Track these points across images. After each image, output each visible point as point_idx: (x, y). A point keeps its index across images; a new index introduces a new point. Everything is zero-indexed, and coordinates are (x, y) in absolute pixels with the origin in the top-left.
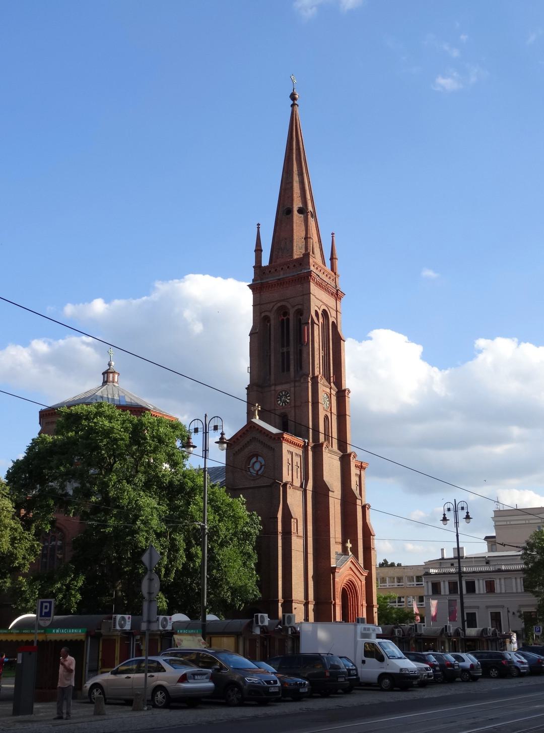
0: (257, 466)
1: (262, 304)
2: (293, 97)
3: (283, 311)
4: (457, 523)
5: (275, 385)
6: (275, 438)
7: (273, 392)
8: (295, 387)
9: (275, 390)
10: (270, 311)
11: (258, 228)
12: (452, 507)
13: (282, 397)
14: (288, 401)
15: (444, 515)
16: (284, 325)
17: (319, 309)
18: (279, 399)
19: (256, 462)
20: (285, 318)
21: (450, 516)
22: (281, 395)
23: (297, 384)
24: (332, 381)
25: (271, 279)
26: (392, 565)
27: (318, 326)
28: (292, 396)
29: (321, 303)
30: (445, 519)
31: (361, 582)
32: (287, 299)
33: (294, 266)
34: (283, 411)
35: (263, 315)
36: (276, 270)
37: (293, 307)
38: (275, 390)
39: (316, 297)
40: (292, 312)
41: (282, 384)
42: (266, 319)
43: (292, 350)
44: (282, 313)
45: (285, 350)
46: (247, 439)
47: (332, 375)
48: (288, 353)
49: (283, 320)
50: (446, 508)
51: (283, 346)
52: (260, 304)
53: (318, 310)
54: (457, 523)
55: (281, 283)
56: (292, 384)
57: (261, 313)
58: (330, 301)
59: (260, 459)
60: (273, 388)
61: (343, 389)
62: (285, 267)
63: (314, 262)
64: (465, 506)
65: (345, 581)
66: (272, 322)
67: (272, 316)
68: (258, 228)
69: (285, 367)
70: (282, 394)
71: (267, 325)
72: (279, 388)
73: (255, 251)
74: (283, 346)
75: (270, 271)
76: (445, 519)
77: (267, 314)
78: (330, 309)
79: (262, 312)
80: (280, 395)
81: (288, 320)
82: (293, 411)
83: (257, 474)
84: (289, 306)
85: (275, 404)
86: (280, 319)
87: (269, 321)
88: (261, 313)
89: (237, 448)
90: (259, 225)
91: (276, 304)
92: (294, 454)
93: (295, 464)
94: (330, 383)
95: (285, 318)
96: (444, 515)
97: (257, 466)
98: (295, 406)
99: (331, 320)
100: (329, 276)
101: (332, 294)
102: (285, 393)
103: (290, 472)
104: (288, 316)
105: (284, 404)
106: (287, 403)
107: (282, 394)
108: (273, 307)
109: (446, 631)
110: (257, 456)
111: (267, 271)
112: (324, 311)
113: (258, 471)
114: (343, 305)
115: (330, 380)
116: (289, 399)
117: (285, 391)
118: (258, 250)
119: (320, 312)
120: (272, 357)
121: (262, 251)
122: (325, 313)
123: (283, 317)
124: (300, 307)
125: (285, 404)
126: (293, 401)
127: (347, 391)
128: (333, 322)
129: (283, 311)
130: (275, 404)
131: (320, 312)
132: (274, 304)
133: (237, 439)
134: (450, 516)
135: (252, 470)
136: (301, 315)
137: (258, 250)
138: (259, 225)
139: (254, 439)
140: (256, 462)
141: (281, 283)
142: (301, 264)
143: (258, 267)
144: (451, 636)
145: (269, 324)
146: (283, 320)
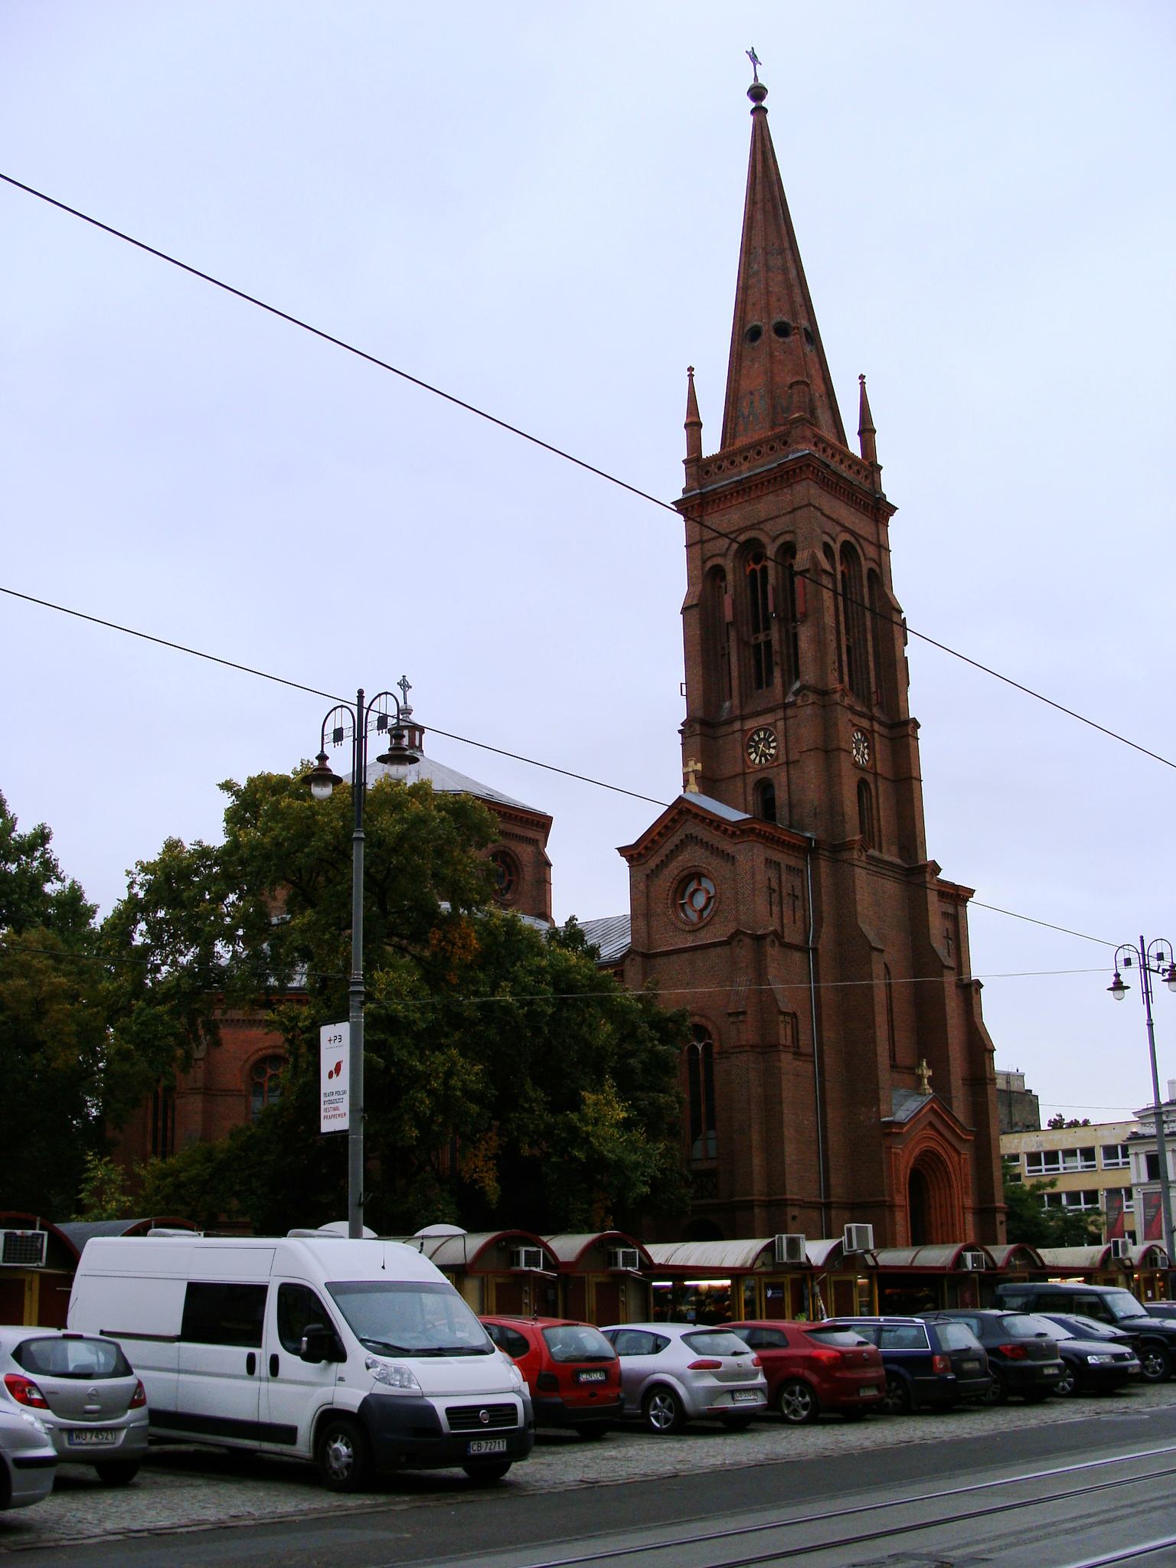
0: (700, 900)
1: (707, 541)
2: (757, 93)
3: (752, 550)
4: (1147, 993)
5: (743, 718)
6: (734, 833)
7: (738, 735)
8: (785, 719)
9: (742, 730)
10: (724, 555)
11: (691, 376)
12: (1134, 956)
13: (757, 743)
15: (1117, 975)
16: (756, 582)
17: (834, 540)
19: (696, 891)
20: (758, 567)
21: (1132, 977)
23: (790, 712)
24: (874, 702)
25: (721, 482)
26: (1074, 1124)
28: (781, 739)
29: (838, 528)
30: (1118, 986)
31: (959, 1154)
32: (759, 523)
33: (772, 448)
34: (761, 775)
35: (709, 564)
36: (732, 463)
37: (774, 540)
38: (742, 730)
39: (823, 514)
40: (771, 551)
41: (758, 714)
43: (775, 635)
45: (762, 637)
46: (676, 839)
47: (873, 689)
48: (768, 644)
49: (754, 571)
50: (1121, 958)
51: (756, 630)
52: (702, 542)
53: (832, 543)
54: (1147, 993)
55: (744, 489)
56: (780, 714)
58: (861, 524)
59: (706, 884)
60: (737, 725)
61: (903, 718)
62: (751, 454)
63: (815, 436)
64: (1166, 951)
65: (917, 1152)
66: (730, 577)
67: (728, 565)
68: (691, 376)
69: (761, 678)
72: (750, 724)
73: (686, 426)
74: (756, 630)
75: (720, 468)
76: (1118, 986)
77: (719, 561)
81: (764, 569)
82: (784, 774)
83: (701, 916)
85: (744, 760)
86: (748, 570)
87: (723, 578)
88: (704, 562)
89: (653, 863)
90: (691, 369)
92: (783, 866)
93: (784, 893)
94: (871, 710)
95: (758, 567)
96: (1117, 975)
97: (700, 900)
98: (787, 763)
99: (866, 565)
100: (855, 468)
101: (866, 507)
103: (775, 909)
109: (1116, 1253)
110: (697, 875)
111: (713, 468)
112: (846, 545)
113: (702, 911)
115: (869, 700)
117: (765, 730)
118: (694, 426)
119: (836, 548)
120: (734, 659)
121: (700, 425)
122: (849, 552)
123: (753, 566)
124: (788, 538)
126: (782, 751)
128: (871, 571)
130: (744, 760)
131: (836, 548)
133: (653, 841)
134: (1132, 977)
135: (690, 912)
136: (794, 557)
137: (694, 426)
138: (691, 369)
139: (690, 838)
140: (696, 891)
141: (744, 489)
142: (785, 443)
143: (695, 462)
144: (1132, 1267)
146: (754, 571)
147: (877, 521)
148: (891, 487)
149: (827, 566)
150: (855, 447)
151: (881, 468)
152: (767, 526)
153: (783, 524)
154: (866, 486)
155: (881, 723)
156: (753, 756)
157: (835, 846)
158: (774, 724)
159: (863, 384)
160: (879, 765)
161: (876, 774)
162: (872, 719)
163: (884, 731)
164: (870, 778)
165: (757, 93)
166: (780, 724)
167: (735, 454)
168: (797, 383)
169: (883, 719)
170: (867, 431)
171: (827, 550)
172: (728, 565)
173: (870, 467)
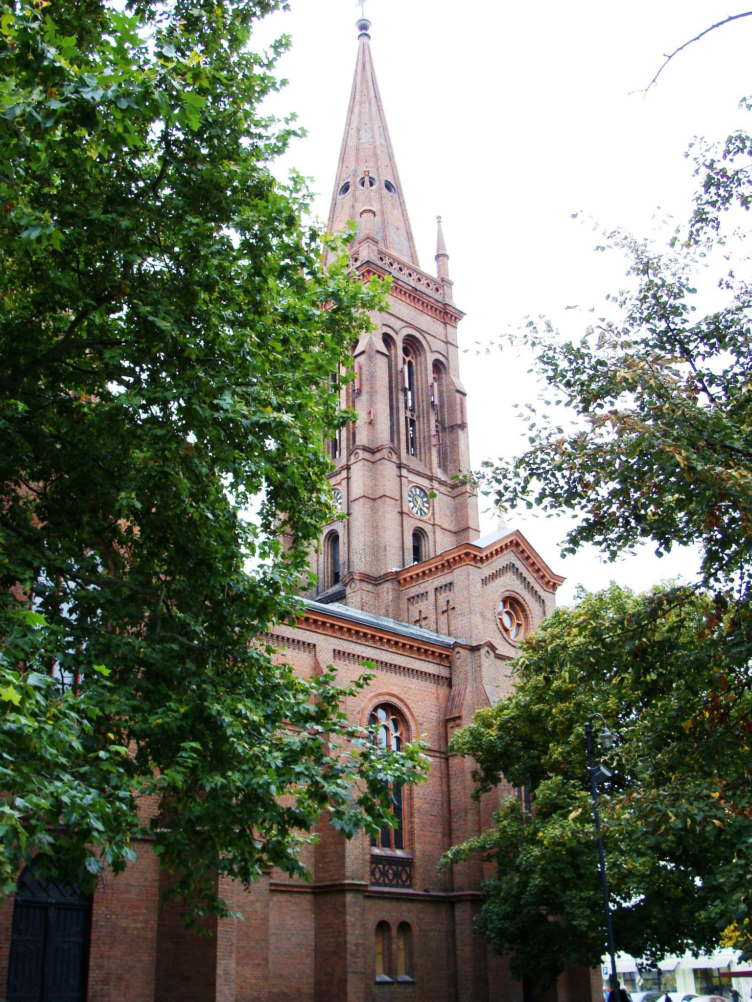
2: (363, 27)
27: (385, 360)
78: (428, 337)
114: (463, 332)
122: (412, 345)
127: (468, 487)
147: (445, 323)
148: (458, 299)
149: (381, 346)
150: (428, 267)
151: (450, 284)
154: (437, 296)
155: (441, 483)
157: (376, 579)
158: (339, 484)
159: (439, 222)
160: (437, 516)
161: (434, 525)
162: (431, 479)
163: (443, 489)
164: (428, 528)
165: (363, 27)
166: (344, 482)
168: (364, 211)
169: (443, 478)
170: (441, 257)
171: (388, 340)
173: (443, 283)
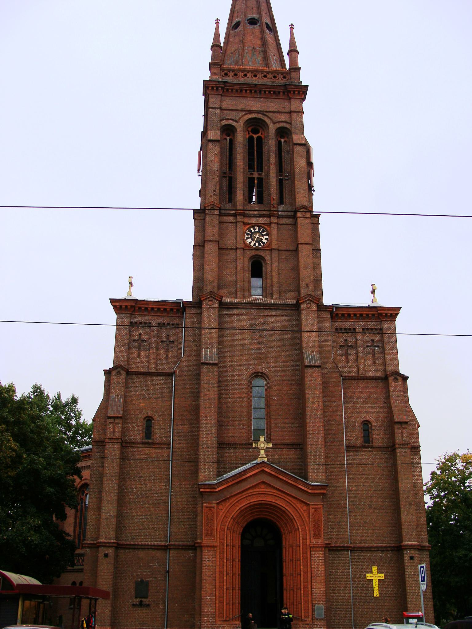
14: (265, 241)
18: (249, 236)
22: (253, 231)
32: (266, 112)
34: (258, 253)
36: (245, 75)
37: (274, 123)
40: (272, 128)
41: (255, 216)
42: (228, 130)
44: (250, 129)
45: (256, 175)
57: (221, 121)
67: (239, 127)
70: (254, 229)
71: (226, 139)
77: (234, 123)
79: (223, 120)
80: (251, 231)
84: (266, 120)
86: (248, 136)
91: (245, 115)
95: (255, 136)
102: (259, 229)
104: (259, 135)
105: (257, 245)
106: (264, 243)
107: (254, 229)
108: (243, 116)
116: (266, 239)
123: (251, 134)
125: (260, 245)
129: (256, 125)
132: (243, 113)
145: (228, 138)
146: (251, 139)
152: (270, 115)
153: (282, 117)
156: (249, 240)
158: (270, 224)
167: (248, 71)
172: (239, 127)
